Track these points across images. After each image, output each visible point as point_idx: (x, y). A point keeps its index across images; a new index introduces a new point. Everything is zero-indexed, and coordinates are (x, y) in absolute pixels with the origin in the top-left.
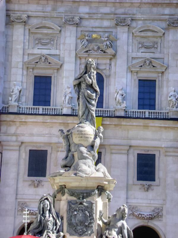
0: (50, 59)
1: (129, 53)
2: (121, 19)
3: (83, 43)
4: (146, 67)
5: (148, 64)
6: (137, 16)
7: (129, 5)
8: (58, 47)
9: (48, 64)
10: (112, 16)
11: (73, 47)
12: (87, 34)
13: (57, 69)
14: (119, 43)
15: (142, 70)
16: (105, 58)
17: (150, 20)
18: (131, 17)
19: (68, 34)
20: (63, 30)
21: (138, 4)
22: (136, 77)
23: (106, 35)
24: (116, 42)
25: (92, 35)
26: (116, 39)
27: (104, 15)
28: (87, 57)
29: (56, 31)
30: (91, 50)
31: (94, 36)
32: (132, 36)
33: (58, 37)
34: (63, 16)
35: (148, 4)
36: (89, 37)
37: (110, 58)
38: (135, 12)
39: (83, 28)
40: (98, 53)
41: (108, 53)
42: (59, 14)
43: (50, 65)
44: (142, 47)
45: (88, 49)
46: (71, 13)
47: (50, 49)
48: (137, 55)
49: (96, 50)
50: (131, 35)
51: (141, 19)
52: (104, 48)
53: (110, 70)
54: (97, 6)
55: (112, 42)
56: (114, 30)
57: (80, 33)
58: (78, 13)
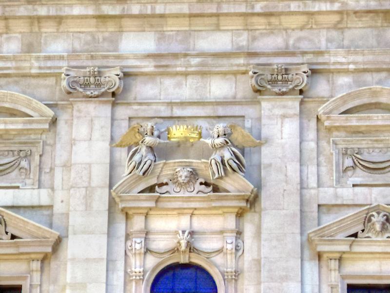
0: (17, 222)
1: (308, 188)
2: (274, 69)
3: (137, 158)
4: (374, 238)
5: (378, 227)
6: (333, 59)
7: (301, 20)
8: (45, 178)
9: (6, 239)
10: (241, 61)
11: (100, 175)
12: (148, 125)
13: (41, 256)
14: (267, 154)
15: (356, 249)
16: (220, 212)
17: (379, 71)
18: (309, 64)
19: (81, 130)
20: (63, 118)
21: (335, 18)
22: (339, 279)
23: (220, 126)
24: (260, 152)
25: (168, 130)
26: (260, 141)
27: (210, 60)
28: (150, 209)
29: (38, 122)
30: (167, 184)
31: (178, 132)
32: (318, 130)
33: (45, 143)
34: (60, 68)
35: (371, 15)
36: (159, 137)
37: (236, 210)
38: (323, 45)
39: (136, 107)
40: (194, 194)
41: (228, 192)
42: (49, 64)
43: (17, 246)
44: (354, 167)
45: (153, 181)
46: (92, 57)
47: (18, 187)
48: (336, 196)
49: (185, 184)
50: (313, 123)
51: (345, 67)
52: (210, 172)
53: (240, 253)
54: (187, 29)
55: (243, 155)
56: (249, 111)
57: (125, 124)
58: (118, 57)
